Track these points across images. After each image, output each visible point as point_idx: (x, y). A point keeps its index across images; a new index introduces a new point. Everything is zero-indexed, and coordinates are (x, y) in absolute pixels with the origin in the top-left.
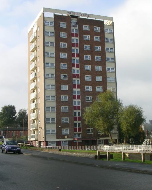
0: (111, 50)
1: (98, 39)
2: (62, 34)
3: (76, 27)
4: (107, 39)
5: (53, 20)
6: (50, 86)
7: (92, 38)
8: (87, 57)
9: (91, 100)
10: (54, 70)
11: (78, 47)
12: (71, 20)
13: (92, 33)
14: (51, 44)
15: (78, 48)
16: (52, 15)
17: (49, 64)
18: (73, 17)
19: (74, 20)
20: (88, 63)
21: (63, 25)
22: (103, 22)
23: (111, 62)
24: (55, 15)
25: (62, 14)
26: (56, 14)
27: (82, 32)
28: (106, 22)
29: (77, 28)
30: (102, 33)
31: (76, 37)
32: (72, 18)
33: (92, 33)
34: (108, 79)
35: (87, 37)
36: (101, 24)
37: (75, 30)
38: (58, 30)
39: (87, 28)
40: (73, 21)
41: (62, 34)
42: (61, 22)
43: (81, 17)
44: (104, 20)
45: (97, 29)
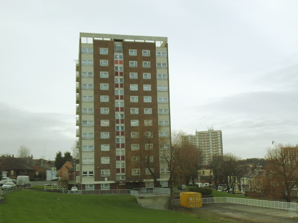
0: (163, 65)
1: (146, 64)
2: (103, 73)
3: (120, 52)
4: (159, 64)
5: (92, 47)
6: (88, 134)
7: (140, 64)
8: (134, 76)
9: (138, 173)
10: (93, 91)
11: (123, 73)
12: (113, 44)
13: (139, 58)
14: (89, 111)
15: (123, 125)
16: (90, 41)
17: (86, 109)
18: (116, 40)
19: (119, 44)
20: (133, 82)
21: (104, 51)
22: (154, 45)
23: (164, 79)
24: (94, 41)
25: (103, 38)
26: (95, 39)
27: (127, 58)
28: (158, 44)
29: (122, 54)
30: (152, 58)
31: (120, 64)
32: (115, 43)
33: (139, 58)
34: (159, 112)
35: (135, 99)
36: (152, 47)
37: (119, 56)
38: (97, 57)
39: (133, 53)
40: (118, 45)
41: (103, 73)
42: (102, 84)
43: (126, 40)
44: (156, 41)
45: (146, 53)
